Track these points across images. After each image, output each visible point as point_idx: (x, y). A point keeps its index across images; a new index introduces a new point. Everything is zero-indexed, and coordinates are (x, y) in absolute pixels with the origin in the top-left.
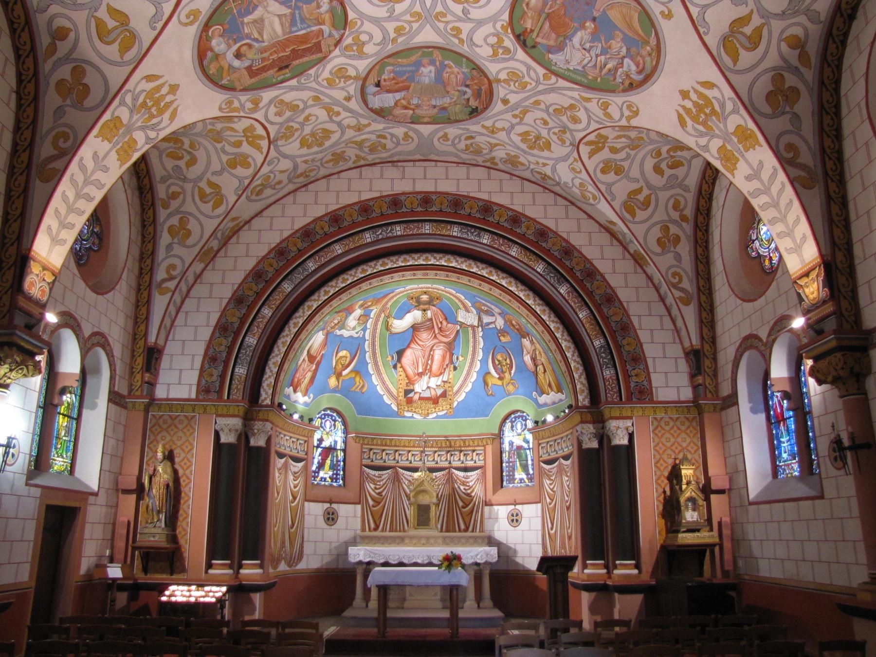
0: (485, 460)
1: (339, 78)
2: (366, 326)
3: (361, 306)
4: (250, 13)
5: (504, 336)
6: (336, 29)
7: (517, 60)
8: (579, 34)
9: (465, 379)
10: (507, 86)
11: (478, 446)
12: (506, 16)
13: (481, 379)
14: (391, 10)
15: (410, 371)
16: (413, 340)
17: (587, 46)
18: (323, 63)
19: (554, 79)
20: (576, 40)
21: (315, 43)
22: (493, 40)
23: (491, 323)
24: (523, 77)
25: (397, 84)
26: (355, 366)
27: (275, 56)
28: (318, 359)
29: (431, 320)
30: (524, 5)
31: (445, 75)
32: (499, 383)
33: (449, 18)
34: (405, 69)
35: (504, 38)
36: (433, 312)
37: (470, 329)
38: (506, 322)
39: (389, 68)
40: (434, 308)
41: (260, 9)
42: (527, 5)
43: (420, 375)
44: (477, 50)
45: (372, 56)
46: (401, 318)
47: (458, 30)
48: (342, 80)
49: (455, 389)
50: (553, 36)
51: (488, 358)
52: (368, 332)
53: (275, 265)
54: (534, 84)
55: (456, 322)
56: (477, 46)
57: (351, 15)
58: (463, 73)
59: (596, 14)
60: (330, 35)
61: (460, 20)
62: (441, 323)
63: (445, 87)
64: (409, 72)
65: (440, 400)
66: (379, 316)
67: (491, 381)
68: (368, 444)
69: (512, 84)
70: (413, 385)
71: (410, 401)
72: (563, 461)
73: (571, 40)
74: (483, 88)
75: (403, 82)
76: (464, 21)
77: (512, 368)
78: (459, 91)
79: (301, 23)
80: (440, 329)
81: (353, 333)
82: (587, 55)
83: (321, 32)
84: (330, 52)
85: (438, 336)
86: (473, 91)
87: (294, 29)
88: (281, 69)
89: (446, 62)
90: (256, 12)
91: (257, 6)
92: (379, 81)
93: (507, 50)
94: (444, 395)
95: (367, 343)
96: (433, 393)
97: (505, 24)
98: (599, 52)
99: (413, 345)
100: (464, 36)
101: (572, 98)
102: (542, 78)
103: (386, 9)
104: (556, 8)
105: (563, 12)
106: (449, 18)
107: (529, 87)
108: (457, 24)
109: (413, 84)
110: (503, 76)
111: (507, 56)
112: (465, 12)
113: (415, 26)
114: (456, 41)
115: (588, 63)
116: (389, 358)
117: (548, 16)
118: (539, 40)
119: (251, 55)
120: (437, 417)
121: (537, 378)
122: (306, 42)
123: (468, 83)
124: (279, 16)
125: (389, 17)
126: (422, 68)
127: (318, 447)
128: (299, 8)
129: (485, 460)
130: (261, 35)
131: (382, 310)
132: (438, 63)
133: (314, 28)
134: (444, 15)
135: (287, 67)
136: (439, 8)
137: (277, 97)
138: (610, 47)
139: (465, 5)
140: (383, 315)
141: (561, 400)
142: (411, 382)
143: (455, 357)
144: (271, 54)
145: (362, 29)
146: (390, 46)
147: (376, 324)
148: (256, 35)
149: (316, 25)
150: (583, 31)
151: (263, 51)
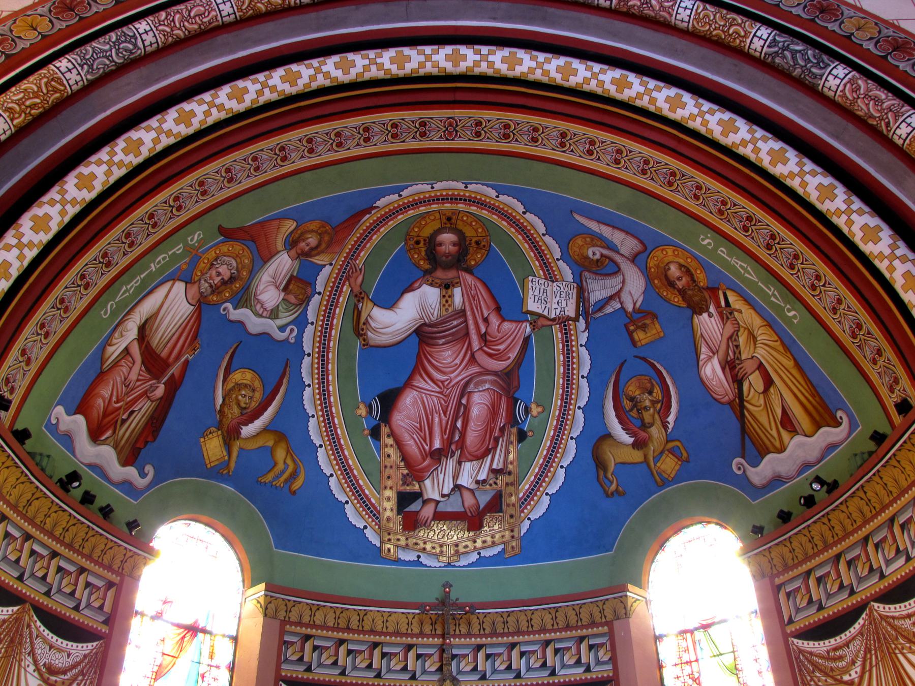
0: (613, 660)
2: (304, 313)
3: (292, 243)
5: (644, 328)
9: (549, 461)
11: (592, 624)
13: (589, 454)
15: (413, 448)
16: (419, 367)
23: (611, 298)
26: (277, 413)
28: (175, 370)
29: (462, 313)
32: (637, 456)
36: (468, 295)
37: (556, 328)
38: (649, 278)
40: (469, 278)
43: (438, 456)
46: (390, 304)
49: (525, 486)
51: (603, 399)
52: (310, 329)
53: (44, 27)
55: (523, 315)
62: (486, 320)
65: (487, 518)
66: (336, 291)
67: (612, 457)
68: (299, 624)
70: (421, 480)
71: (411, 523)
72: (880, 608)
77: (669, 407)
80: (483, 338)
81: (271, 326)
85: (481, 358)
94: (496, 505)
95: (307, 361)
96: (469, 500)
99: (419, 382)
116: (363, 411)
120: (482, 561)
121: (741, 418)
127: (158, 616)
129: (613, 660)
131: (345, 275)
140: (346, 289)
141: (831, 447)
142: (415, 473)
143: (520, 408)
147: (329, 314)
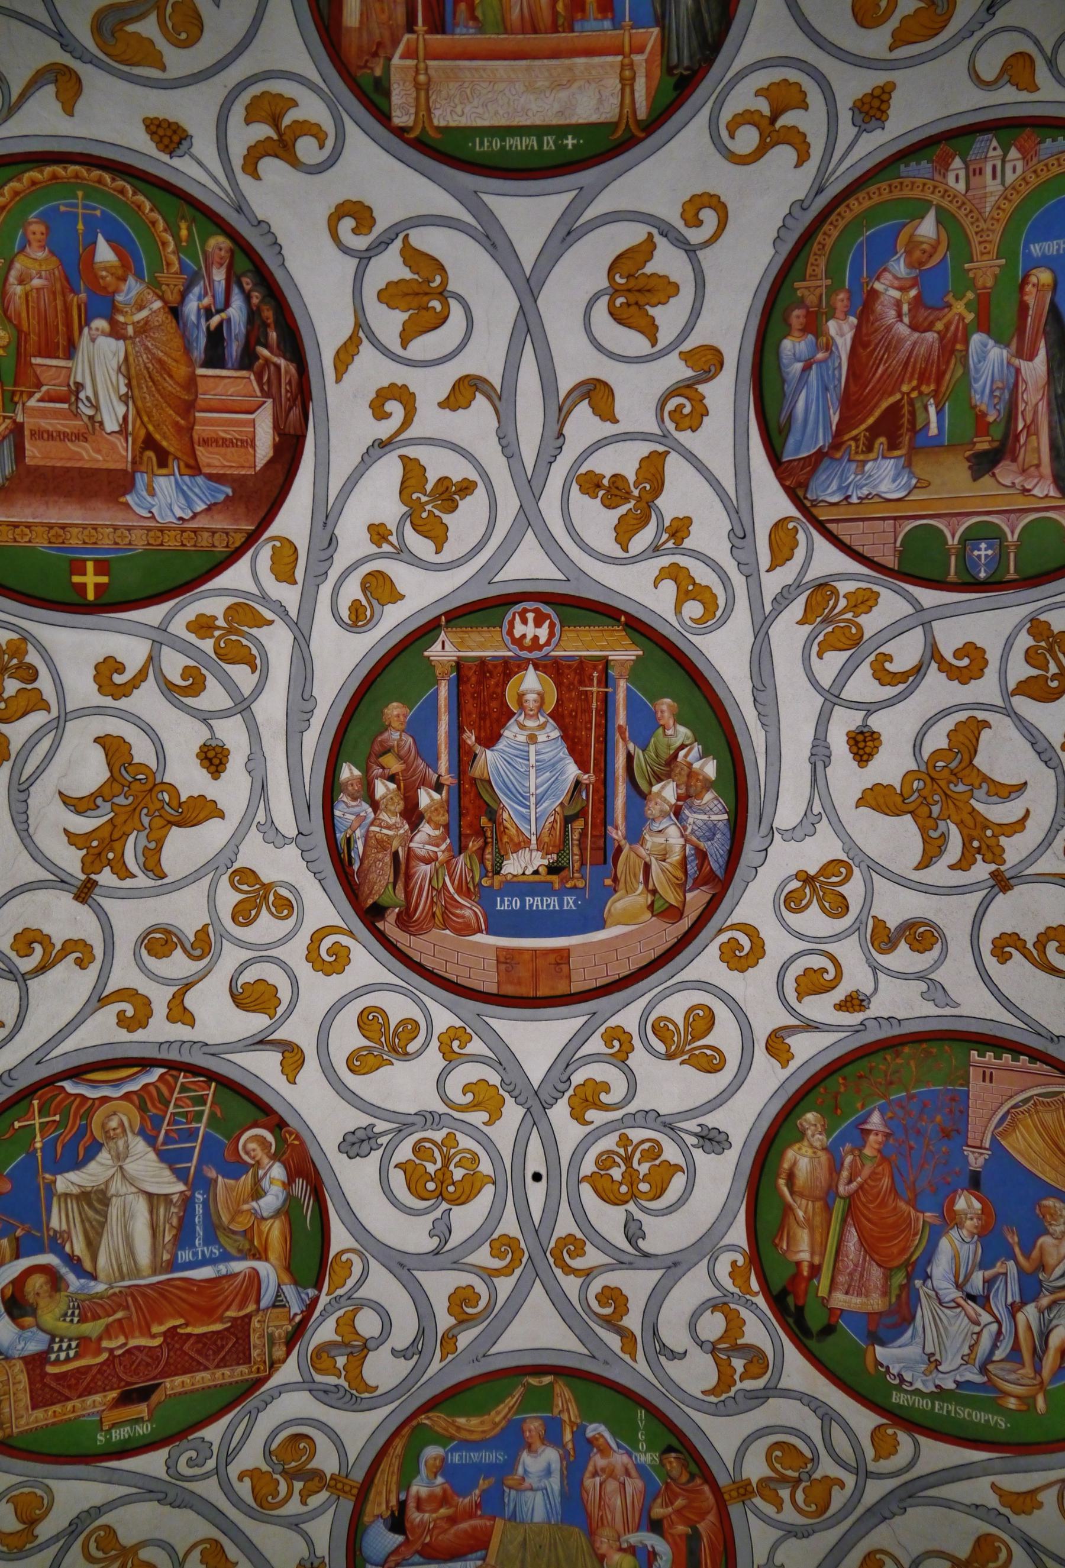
1: (291, 1476)
4: (78, 1165)
6: (296, 1283)
7: (787, 1394)
8: (944, 1244)
10: (769, 1510)
12: (738, 1234)
14: (442, 1227)
17: (978, 1280)
18: (251, 1402)
19: (904, 1439)
20: (941, 1269)
21: (234, 1320)
22: (713, 1326)
24: (815, 1460)
25: (452, 1520)
27: (115, 1343)
30: (782, 1182)
31: (588, 1482)
33: (593, 1257)
34: (475, 1457)
35: (745, 1313)
39: (432, 1452)
41: (104, 1156)
42: (791, 1177)
44: (673, 1368)
45: (388, 1397)
47: (614, 1297)
48: (298, 1485)
50: (876, 1273)
54: (850, 1480)
56: (674, 1356)
57: (340, 1238)
58: (640, 1468)
59: (976, 1161)
60: (279, 1302)
61: (622, 1264)
63: (591, 1534)
64: (489, 1470)
69: (785, 1493)
73: (927, 1277)
74: (702, 1527)
75: (471, 1515)
76: (630, 1266)
78: (632, 1550)
79: (207, 1242)
82: (985, 1318)
83: (254, 1279)
84: (274, 1365)
86: (674, 1546)
87: (185, 1256)
88: (127, 1398)
89: (593, 1430)
90: (92, 1166)
91: (101, 1146)
92: (402, 1505)
93: (756, 1360)
97: (740, 1263)
98: (1013, 1294)
100: (632, 1321)
101: (976, 1509)
102: (870, 1453)
103: (427, 1221)
104: (866, 1172)
105: (886, 1182)
106: (593, 1257)
107: (838, 1499)
108: (613, 1279)
109: (499, 1523)
110: (755, 1469)
111: (760, 1383)
112: (633, 1232)
113: (505, 1285)
114: (613, 1341)
115: (995, 1347)
117: (851, 1210)
118: (840, 1300)
119: (50, 1314)
122: (209, 1313)
123: (658, 1511)
124: (150, 1196)
125: (436, 1252)
126: (525, 1457)
128: (209, 1185)
130: (93, 1247)
132: (568, 1436)
133: (238, 1266)
134: (573, 1245)
135: (144, 1394)
136: (566, 1225)
137: (99, 1511)
138: (1042, 1266)
139: (631, 1206)
144: (107, 1333)
145: (362, 1293)
146: (436, 1365)
148: (78, 1247)
149: (243, 1256)
150: (954, 1233)
151: (87, 1309)
